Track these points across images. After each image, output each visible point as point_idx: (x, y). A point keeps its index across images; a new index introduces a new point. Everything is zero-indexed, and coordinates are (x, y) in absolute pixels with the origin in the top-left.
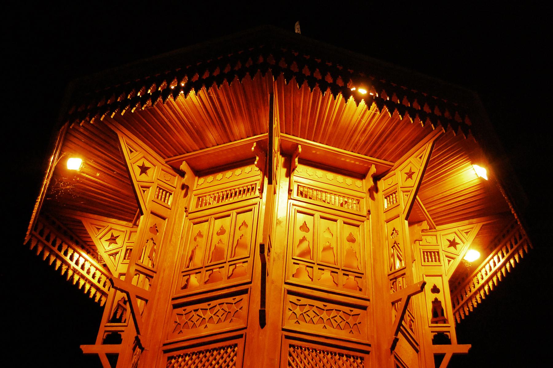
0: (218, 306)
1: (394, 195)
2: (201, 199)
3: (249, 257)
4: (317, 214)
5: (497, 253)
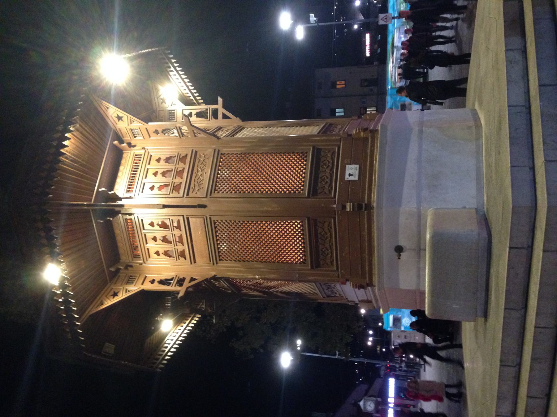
3: (169, 219)
4: (144, 181)
5: (170, 76)
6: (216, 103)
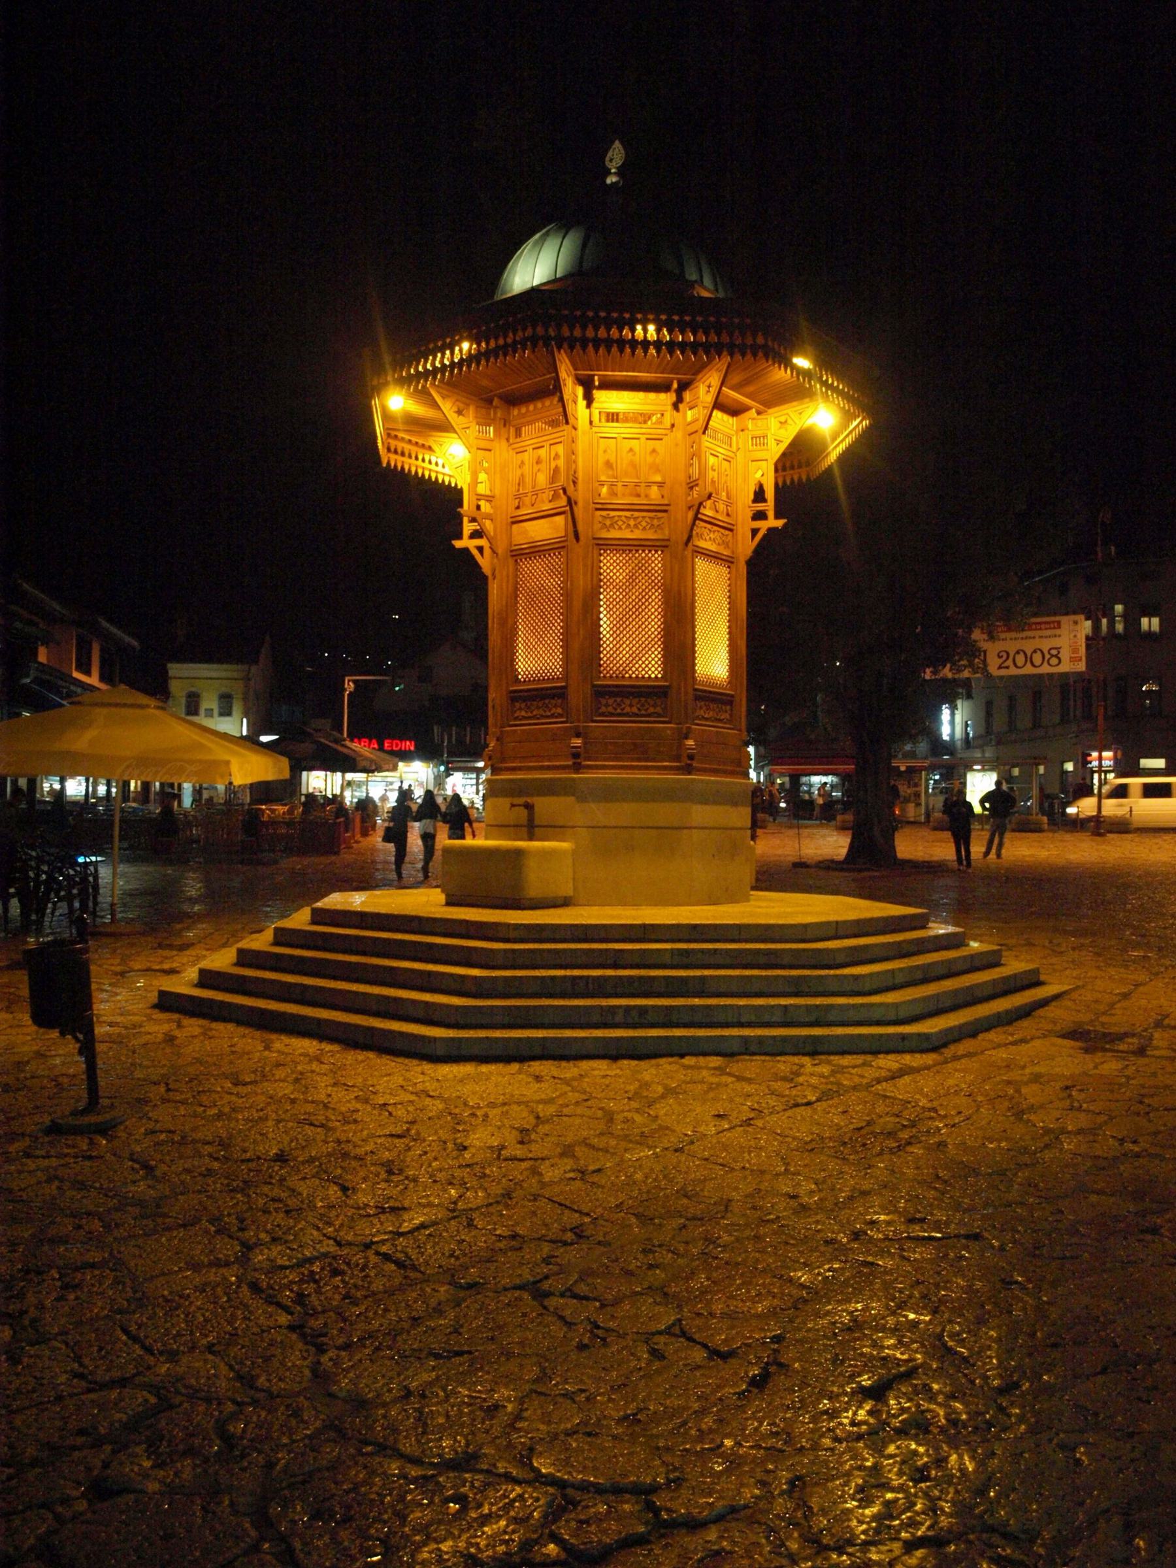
6: (777, 517)
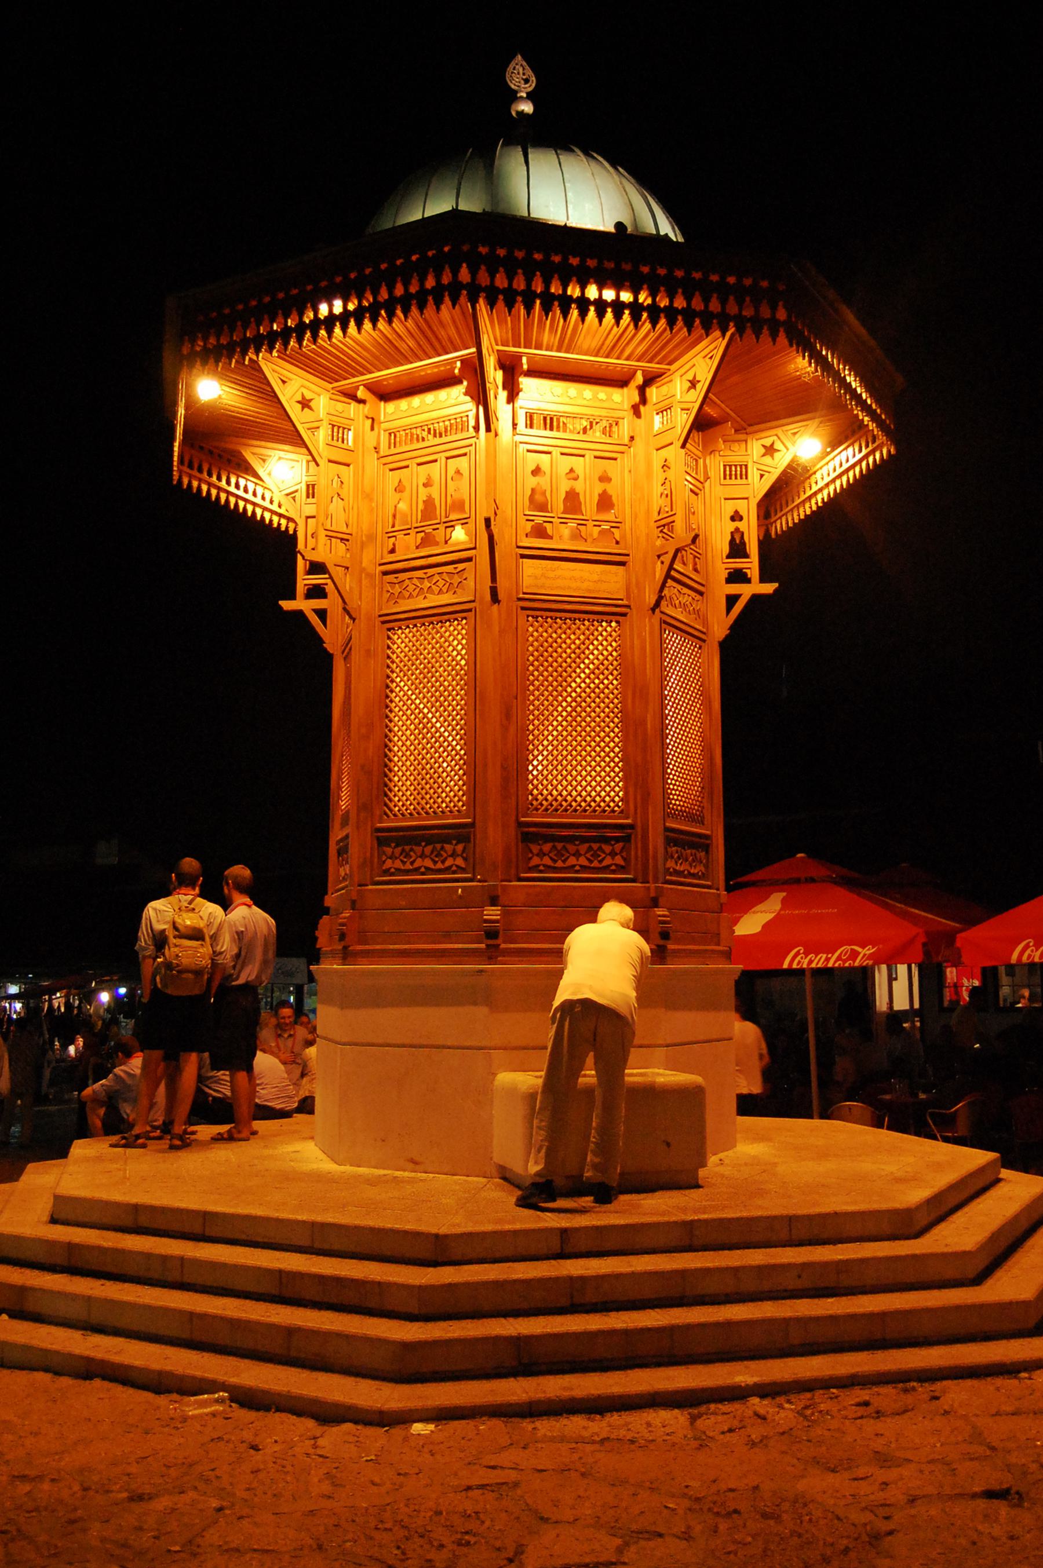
0: (437, 575)
1: (669, 411)
2: (393, 435)
4: (556, 452)
